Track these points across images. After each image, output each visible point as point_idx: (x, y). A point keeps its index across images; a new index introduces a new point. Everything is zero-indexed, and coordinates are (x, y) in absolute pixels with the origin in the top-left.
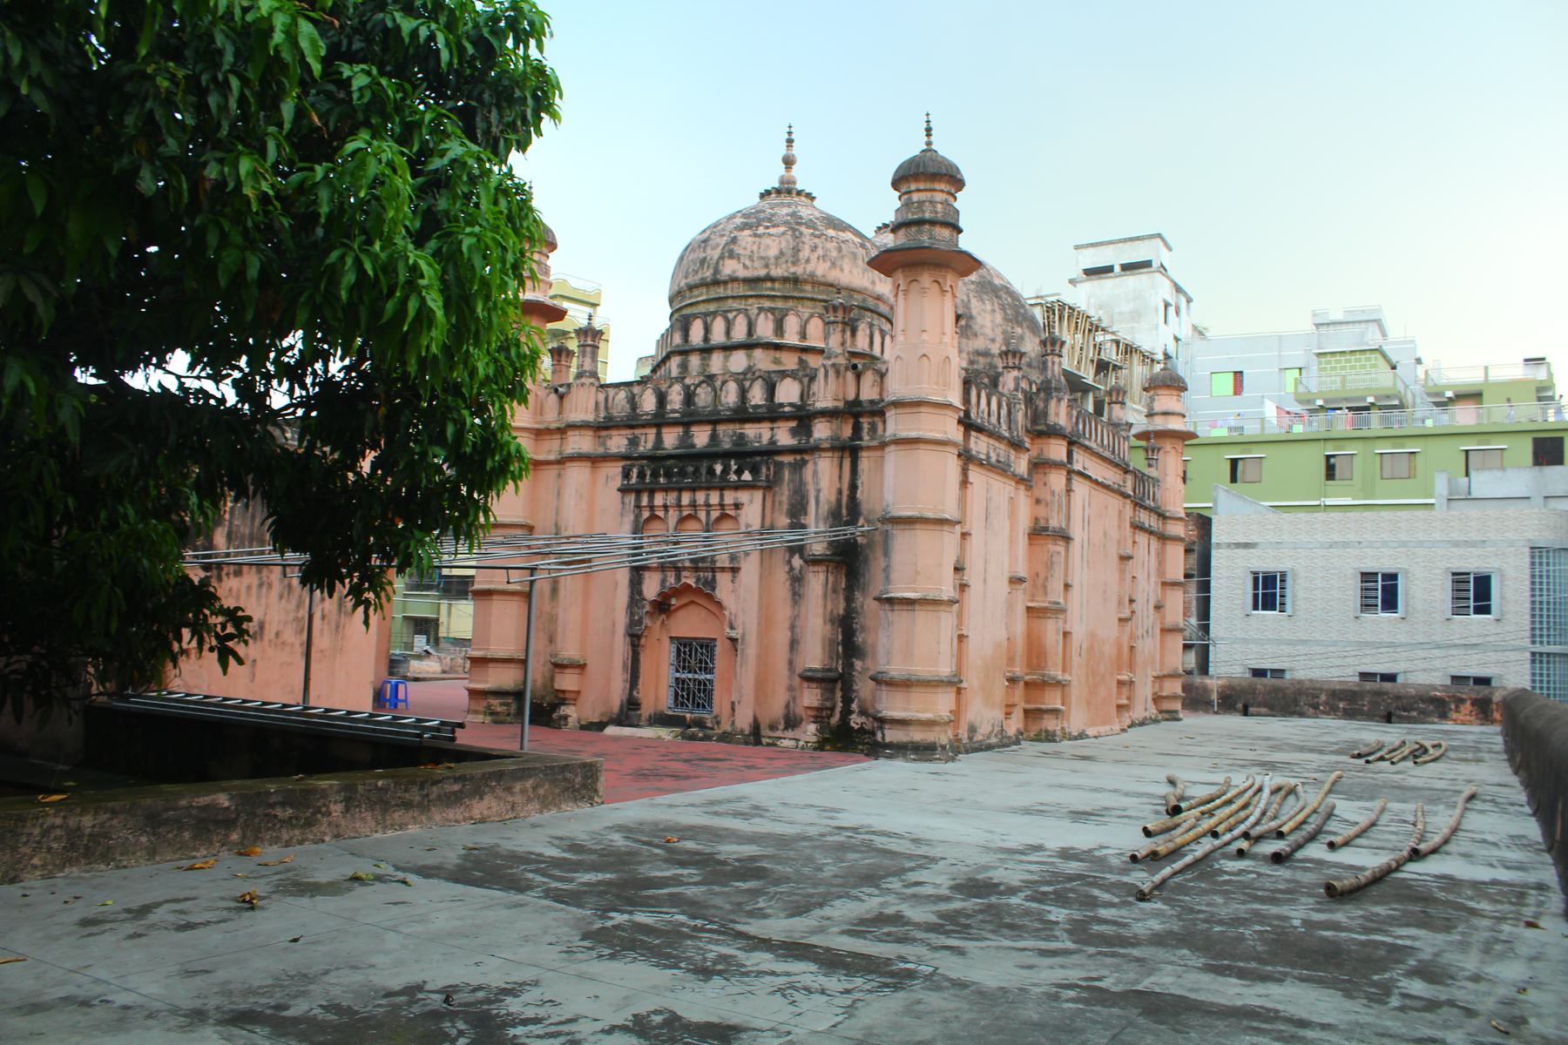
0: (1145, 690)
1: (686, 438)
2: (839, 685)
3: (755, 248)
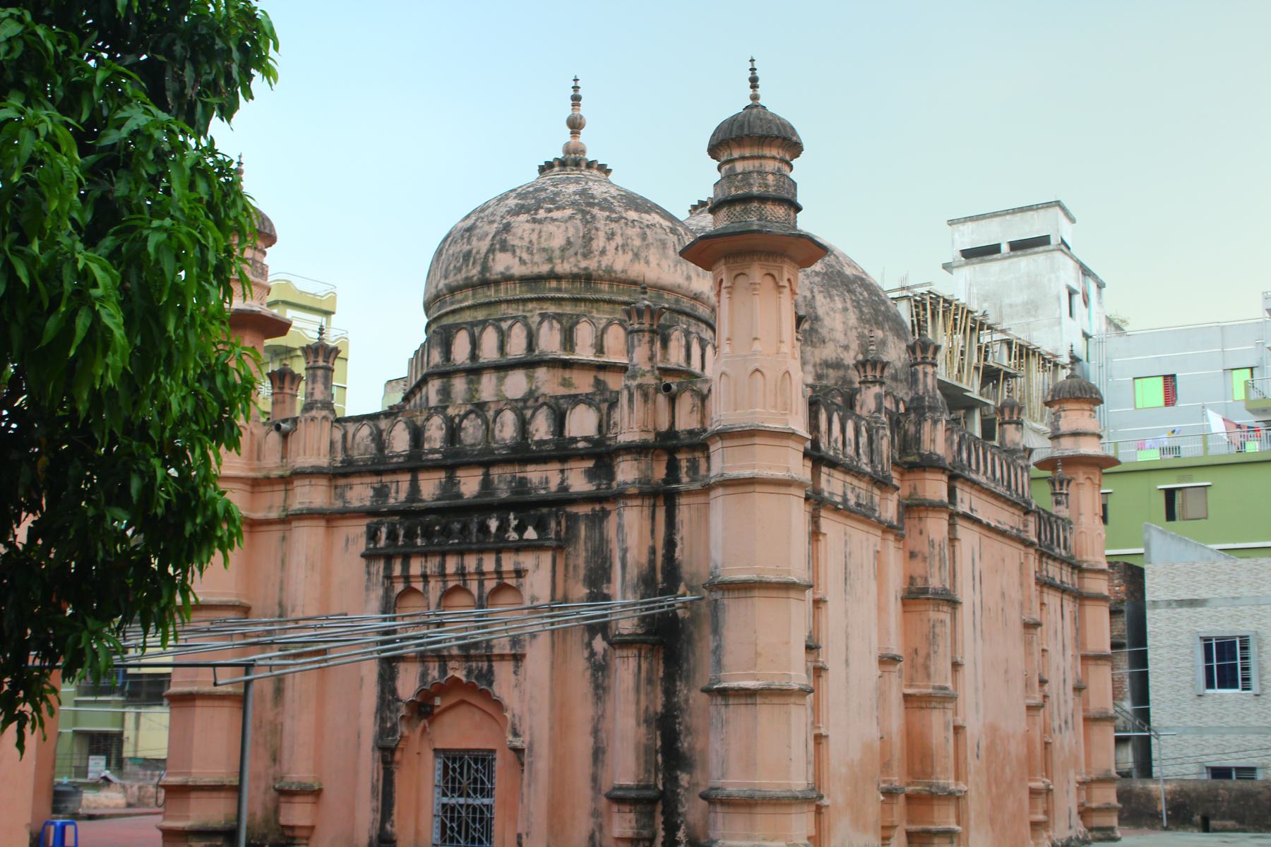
0: (1067, 801)
1: (450, 486)
2: (660, 808)
3: (534, 237)
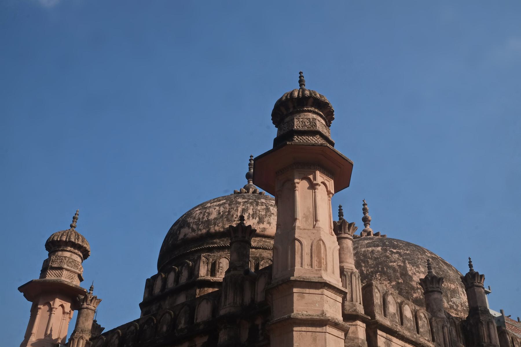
3: (201, 216)
